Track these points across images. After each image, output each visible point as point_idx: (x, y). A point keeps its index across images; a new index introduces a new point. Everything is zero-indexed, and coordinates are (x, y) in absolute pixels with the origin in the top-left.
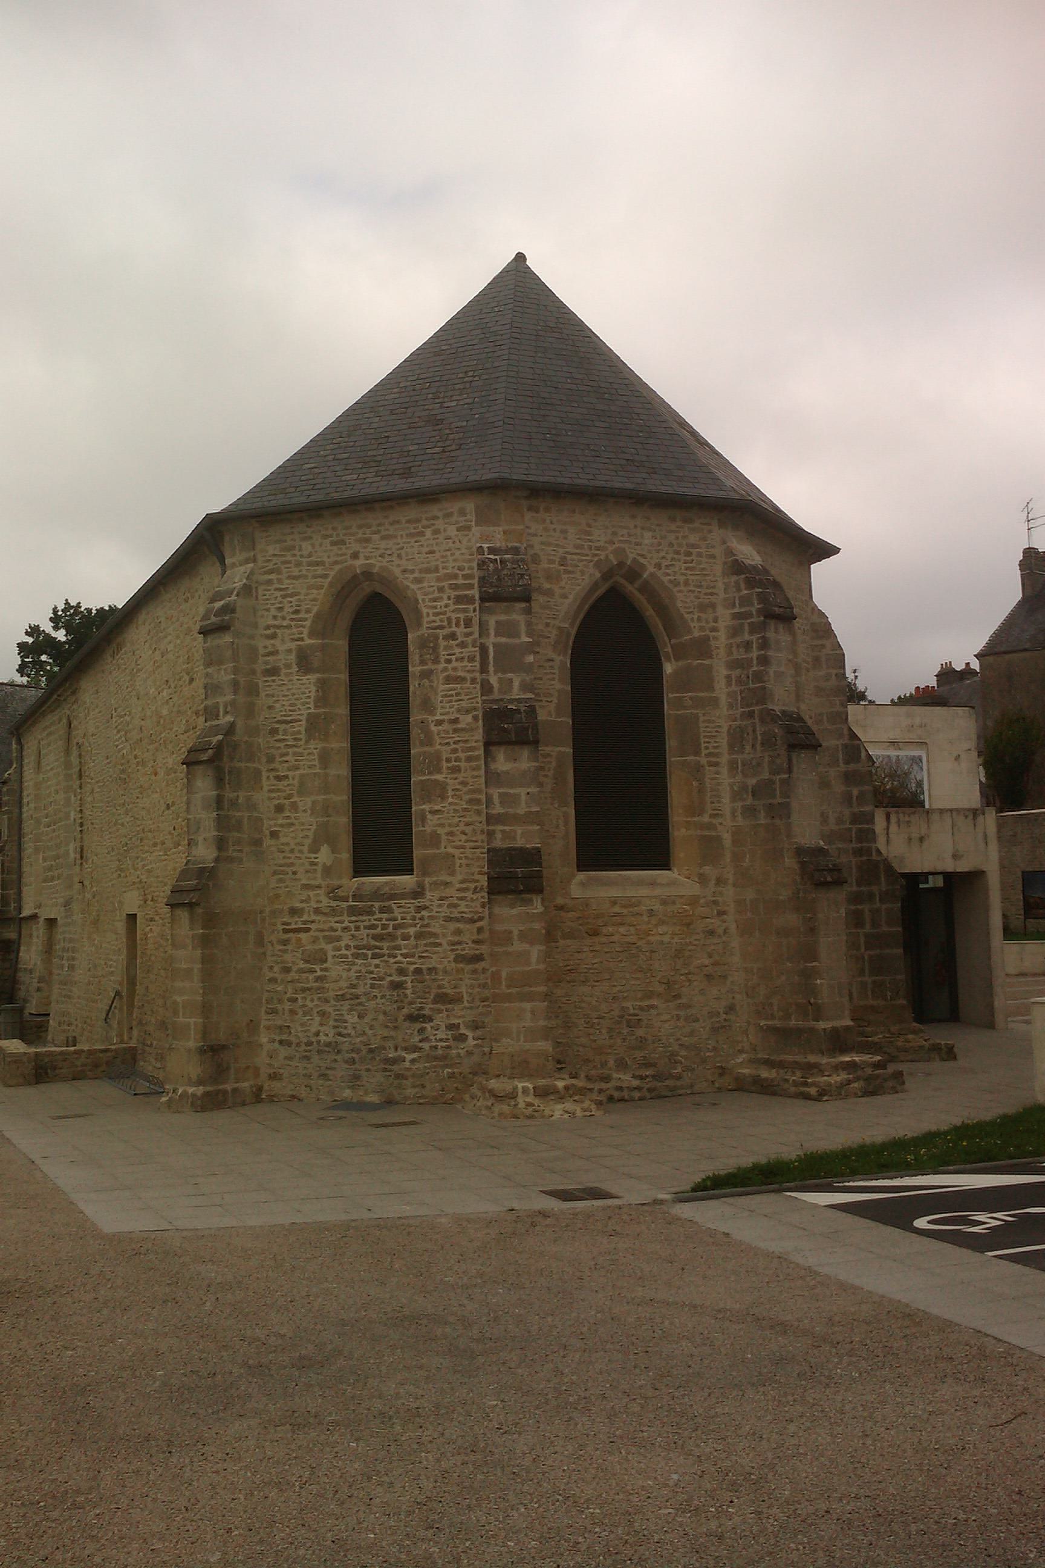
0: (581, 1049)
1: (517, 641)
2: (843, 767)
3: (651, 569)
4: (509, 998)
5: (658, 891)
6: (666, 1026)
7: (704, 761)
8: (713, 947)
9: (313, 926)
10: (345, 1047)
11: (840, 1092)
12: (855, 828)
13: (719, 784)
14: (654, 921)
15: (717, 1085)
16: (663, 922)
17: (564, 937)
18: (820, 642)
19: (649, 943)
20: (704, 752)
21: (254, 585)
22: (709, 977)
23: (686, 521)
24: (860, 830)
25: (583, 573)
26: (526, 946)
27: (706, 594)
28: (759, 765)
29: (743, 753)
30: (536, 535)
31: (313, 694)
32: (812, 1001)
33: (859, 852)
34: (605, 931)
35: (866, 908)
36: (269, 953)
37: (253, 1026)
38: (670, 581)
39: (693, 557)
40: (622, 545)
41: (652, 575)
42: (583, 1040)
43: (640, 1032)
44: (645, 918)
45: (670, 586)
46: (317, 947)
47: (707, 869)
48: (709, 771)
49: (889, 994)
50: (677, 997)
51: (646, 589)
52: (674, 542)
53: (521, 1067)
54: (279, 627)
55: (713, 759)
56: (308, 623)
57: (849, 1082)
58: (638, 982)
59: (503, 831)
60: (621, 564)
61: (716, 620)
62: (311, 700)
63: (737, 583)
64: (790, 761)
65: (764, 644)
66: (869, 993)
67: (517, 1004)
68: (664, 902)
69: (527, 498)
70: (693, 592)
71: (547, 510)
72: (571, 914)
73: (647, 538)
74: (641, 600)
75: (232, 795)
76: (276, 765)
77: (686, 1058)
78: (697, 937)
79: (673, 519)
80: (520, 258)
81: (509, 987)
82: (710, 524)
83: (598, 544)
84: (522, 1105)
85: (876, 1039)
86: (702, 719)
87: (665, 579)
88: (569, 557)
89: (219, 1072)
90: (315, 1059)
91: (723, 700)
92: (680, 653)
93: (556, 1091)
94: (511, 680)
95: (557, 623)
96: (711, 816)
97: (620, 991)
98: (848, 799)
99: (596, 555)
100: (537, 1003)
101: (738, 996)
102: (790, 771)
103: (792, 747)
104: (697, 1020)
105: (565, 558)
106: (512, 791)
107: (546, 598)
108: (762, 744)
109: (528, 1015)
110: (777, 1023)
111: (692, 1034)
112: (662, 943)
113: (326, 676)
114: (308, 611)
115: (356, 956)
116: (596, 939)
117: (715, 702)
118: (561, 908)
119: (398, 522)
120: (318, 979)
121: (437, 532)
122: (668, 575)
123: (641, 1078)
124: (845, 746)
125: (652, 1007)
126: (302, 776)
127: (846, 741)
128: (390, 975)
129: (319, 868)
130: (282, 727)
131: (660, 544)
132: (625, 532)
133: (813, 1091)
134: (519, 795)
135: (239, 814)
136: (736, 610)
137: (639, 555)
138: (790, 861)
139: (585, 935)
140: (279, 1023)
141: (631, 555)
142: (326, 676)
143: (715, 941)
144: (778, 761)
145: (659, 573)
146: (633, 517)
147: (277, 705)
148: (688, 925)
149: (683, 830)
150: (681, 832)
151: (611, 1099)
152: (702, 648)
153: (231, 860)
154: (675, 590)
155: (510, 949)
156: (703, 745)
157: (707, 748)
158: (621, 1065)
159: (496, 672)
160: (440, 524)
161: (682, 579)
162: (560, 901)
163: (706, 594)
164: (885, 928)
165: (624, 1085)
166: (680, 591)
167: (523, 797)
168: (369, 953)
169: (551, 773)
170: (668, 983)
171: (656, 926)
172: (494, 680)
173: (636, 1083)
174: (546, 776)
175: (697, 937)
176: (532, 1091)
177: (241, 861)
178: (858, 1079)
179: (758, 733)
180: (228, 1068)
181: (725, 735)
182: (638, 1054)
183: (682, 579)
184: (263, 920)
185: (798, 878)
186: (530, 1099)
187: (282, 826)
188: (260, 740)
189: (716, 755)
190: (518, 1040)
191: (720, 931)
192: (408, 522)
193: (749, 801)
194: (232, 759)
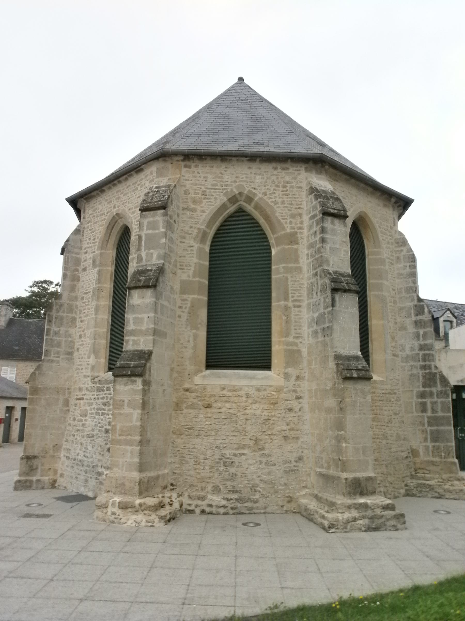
0: (189, 478)
1: (157, 231)
2: (414, 318)
3: (260, 195)
4: (119, 442)
5: (254, 382)
6: (252, 467)
7: (290, 304)
8: (290, 419)
9: (85, 397)
10: (85, 463)
11: (347, 526)
12: (421, 353)
13: (300, 318)
14: (250, 401)
15: (285, 508)
16: (256, 402)
17: (187, 408)
18: (400, 249)
19: (245, 414)
20: (291, 299)
21: (82, 230)
22: (286, 438)
23: (283, 169)
24: (425, 355)
25: (216, 199)
26: (131, 410)
27: (296, 208)
28: (319, 304)
29: (312, 298)
30: (188, 180)
31: (95, 278)
32: (341, 458)
33: (424, 367)
34: (215, 405)
35: (428, 401)
36: (71, 410)
37: (57, 447)
38: (273, 202)
39: (288, 188)
40: (241, 183)
41: (260, 199)
42: (192, 472)
43: (232, 470)
44: (244, 399)
45: (273, 204)
46: (85, 408)
47: (290, 370)
48: (294, 311)
49: (443, 454)
50: (262, 449)
51: (257, 207)
52: (276, 181)
53: (120, 488)
54: (88, 248)
55: (297, 304)
56: (97, 244)
57: (355, 519)
58: (235, 438)
59: (134, 340)
60: (240, 194)
61: (302, 223)
62: (95, 281)
63: (311, 199)
64: (333, 300)
65: (323, 230)
66: (431, 453)
67: (123, 447)
68: (258, 390)
69: (183, 160)
70: (287, 207)
71: (196, 166)
72: (193, 394)
73: (258, 179)
74: (257, 215)
75: (57, 329)
76: (82, 315)
77: (264, 489)
78: (280, 412)
79: (276, 169)
80: (241, 79)
81: (120, 435)
82: (299, 170)
83: (227, 183)
84: (109, 513)
85: (431, 483)
86: (290, 279)
87: (269, 201)
88: (208, 190)
89: (31, 470)
90: (76, 467)
91: (305, 269)
92: (279, 241)
93: (134, 507)
94: (152, 254)
95: (197, 226)
96: (294, 337)
97: (221, 443)
98: (417, 336)
99: (225, 189)
100: (134, 447)
101: (305, 451)
102: (333, 305)
103: (335, 290)
104: (275, 465)
105: (205, 191)
106: (140, 316)
107: (191, 213)
108: (321, 291)
109: (129, 455)
110: (324, 471)
111: (269, 473)
112: (255, 415)
113: (101, 268)
114: (98, 238)
115: (97, 414)
116: (208, 410)
117: (299, 270)
118: (187, 390)
119: (129, 186)
120: (83, 425)
121: (142, 186)
122: (271, 198)
123: (228, 500)
124: (416, 306)
125: (243, 454)
126: (88, 319)
127: (416, 302)
128: (106, 425)
129: (90, 367)
130: (85, 296)
131: (266, 182)
132: (244, 176)
133: (326, 523)
134: (143, 318)
135: (60, 339)
136: (311, 215)
137: (252, 188)
138: (332, 364)
139: (202, 407)
140: (68, 447)
141: (247, 189)
142: (101, 268)
143: (293, 415)
144: (327, 300)
145: (265, 198)
146: (250, 168)
147: (85, 285)
148: (274, 404)
149: (277, 346)
150: (277, 348)
151: (203, 512)
152: (293, 239)
153: (52, 361)
154: (275, 207)
155: (122, 411)
156: (290, 295)
157: (293, 297)
158: (216, 490)
159: (145, 250)
160: (143, 182)
161: (280, 200)
162: (187, 386)
163: (296, 208)
164: (440, 414)
165: (214, 504)
166: (278, 207)
167: (146, 319)
168: (101, 412)
169: (186, 310)
170: (256, 440)
171: (251, 404)
172: (143, 255)
173: (224, 503)
174: (183, 312)
175: (280, 412)
176: (117, 504)
177: (58, 362)
178: (364, 517)
179: (319, 284)
180: (37, 469)
181: (306, 289)
182: (229, 484)
183: (280, 200)
184: (70, 393)
185: (335, 374)
186: (116, 510)
187: (80, 345)
188: (78, 303)
189: (299, 301)
190: (122, 470)
191: (297, 409)
192: (133, 184)
193: (315, 327)
194: (58, 312)
